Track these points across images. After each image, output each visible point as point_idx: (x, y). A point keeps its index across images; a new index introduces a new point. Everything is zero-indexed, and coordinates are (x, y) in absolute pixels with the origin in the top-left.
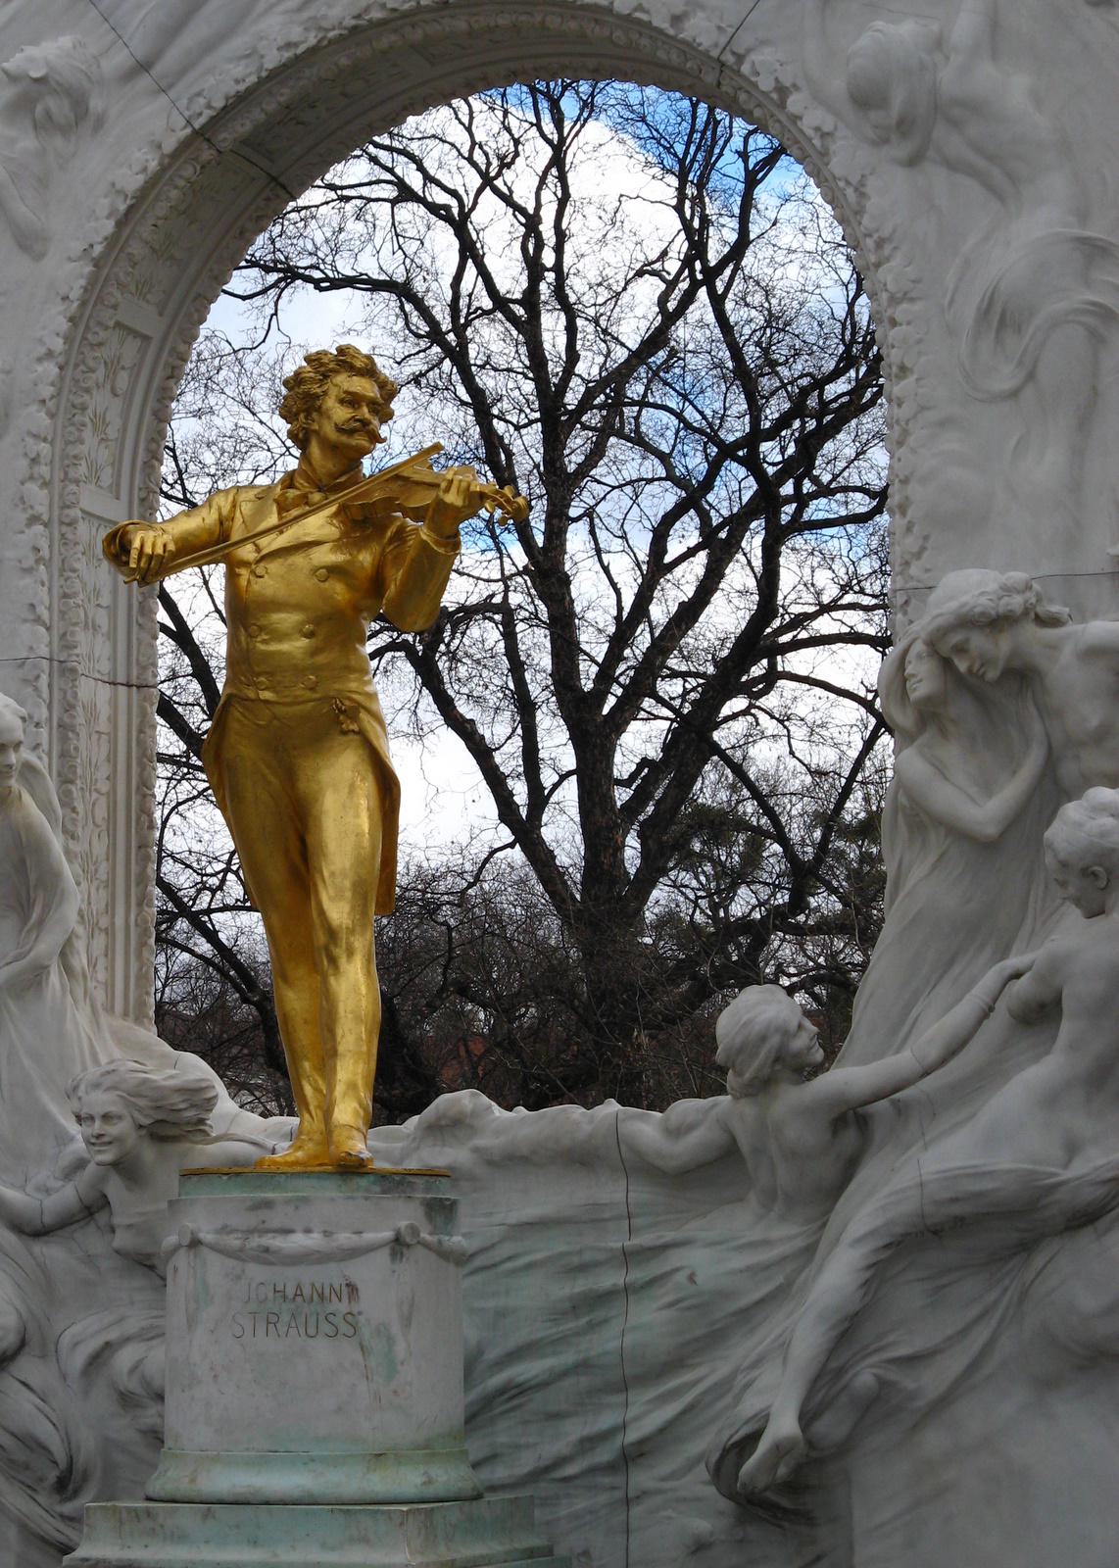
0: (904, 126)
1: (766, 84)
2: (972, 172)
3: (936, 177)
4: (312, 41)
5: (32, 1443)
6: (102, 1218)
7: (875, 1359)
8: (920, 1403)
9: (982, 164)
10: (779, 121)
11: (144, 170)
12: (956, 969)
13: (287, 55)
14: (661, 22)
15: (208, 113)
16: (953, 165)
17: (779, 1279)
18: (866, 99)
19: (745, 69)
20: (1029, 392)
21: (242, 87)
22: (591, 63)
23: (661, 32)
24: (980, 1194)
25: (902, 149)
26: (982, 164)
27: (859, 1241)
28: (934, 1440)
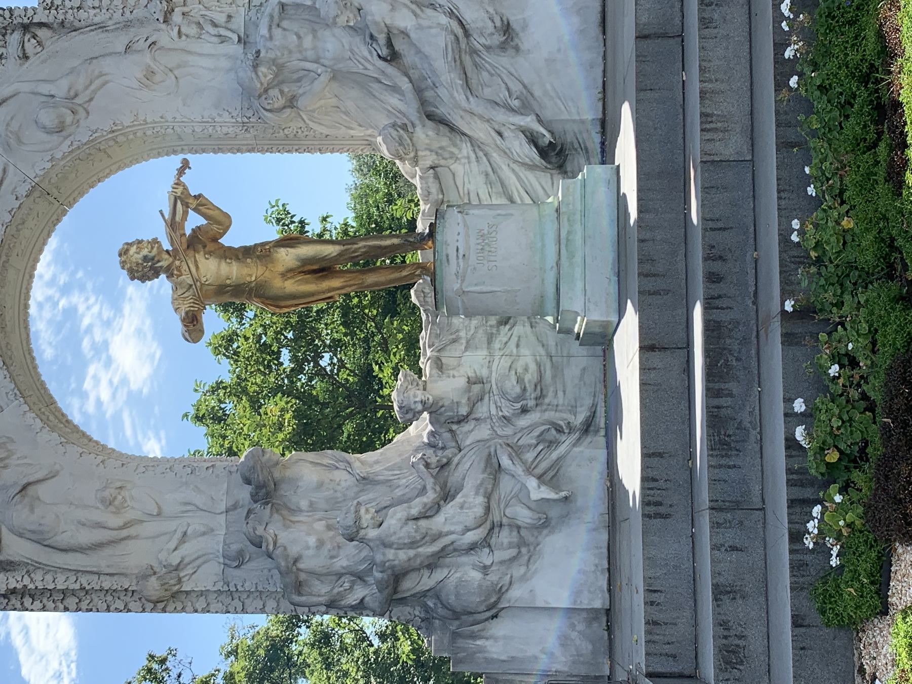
2: (95, 92)
3: (92, 107)
5: (540, 438)
7: (509, 101)
8: (524, 91)
9: (93, 87)
11: (34, 418)
12: (377, 94)
15: (16, 391)
16: (91, 100)
17: (481, 154)
19: (42, 173)
20: (176, 72)
21: (8, 376)
22: (27, 276)
24: (453, 50)
25: (82, 113)
27: (468, 99)
28: (537, 93)
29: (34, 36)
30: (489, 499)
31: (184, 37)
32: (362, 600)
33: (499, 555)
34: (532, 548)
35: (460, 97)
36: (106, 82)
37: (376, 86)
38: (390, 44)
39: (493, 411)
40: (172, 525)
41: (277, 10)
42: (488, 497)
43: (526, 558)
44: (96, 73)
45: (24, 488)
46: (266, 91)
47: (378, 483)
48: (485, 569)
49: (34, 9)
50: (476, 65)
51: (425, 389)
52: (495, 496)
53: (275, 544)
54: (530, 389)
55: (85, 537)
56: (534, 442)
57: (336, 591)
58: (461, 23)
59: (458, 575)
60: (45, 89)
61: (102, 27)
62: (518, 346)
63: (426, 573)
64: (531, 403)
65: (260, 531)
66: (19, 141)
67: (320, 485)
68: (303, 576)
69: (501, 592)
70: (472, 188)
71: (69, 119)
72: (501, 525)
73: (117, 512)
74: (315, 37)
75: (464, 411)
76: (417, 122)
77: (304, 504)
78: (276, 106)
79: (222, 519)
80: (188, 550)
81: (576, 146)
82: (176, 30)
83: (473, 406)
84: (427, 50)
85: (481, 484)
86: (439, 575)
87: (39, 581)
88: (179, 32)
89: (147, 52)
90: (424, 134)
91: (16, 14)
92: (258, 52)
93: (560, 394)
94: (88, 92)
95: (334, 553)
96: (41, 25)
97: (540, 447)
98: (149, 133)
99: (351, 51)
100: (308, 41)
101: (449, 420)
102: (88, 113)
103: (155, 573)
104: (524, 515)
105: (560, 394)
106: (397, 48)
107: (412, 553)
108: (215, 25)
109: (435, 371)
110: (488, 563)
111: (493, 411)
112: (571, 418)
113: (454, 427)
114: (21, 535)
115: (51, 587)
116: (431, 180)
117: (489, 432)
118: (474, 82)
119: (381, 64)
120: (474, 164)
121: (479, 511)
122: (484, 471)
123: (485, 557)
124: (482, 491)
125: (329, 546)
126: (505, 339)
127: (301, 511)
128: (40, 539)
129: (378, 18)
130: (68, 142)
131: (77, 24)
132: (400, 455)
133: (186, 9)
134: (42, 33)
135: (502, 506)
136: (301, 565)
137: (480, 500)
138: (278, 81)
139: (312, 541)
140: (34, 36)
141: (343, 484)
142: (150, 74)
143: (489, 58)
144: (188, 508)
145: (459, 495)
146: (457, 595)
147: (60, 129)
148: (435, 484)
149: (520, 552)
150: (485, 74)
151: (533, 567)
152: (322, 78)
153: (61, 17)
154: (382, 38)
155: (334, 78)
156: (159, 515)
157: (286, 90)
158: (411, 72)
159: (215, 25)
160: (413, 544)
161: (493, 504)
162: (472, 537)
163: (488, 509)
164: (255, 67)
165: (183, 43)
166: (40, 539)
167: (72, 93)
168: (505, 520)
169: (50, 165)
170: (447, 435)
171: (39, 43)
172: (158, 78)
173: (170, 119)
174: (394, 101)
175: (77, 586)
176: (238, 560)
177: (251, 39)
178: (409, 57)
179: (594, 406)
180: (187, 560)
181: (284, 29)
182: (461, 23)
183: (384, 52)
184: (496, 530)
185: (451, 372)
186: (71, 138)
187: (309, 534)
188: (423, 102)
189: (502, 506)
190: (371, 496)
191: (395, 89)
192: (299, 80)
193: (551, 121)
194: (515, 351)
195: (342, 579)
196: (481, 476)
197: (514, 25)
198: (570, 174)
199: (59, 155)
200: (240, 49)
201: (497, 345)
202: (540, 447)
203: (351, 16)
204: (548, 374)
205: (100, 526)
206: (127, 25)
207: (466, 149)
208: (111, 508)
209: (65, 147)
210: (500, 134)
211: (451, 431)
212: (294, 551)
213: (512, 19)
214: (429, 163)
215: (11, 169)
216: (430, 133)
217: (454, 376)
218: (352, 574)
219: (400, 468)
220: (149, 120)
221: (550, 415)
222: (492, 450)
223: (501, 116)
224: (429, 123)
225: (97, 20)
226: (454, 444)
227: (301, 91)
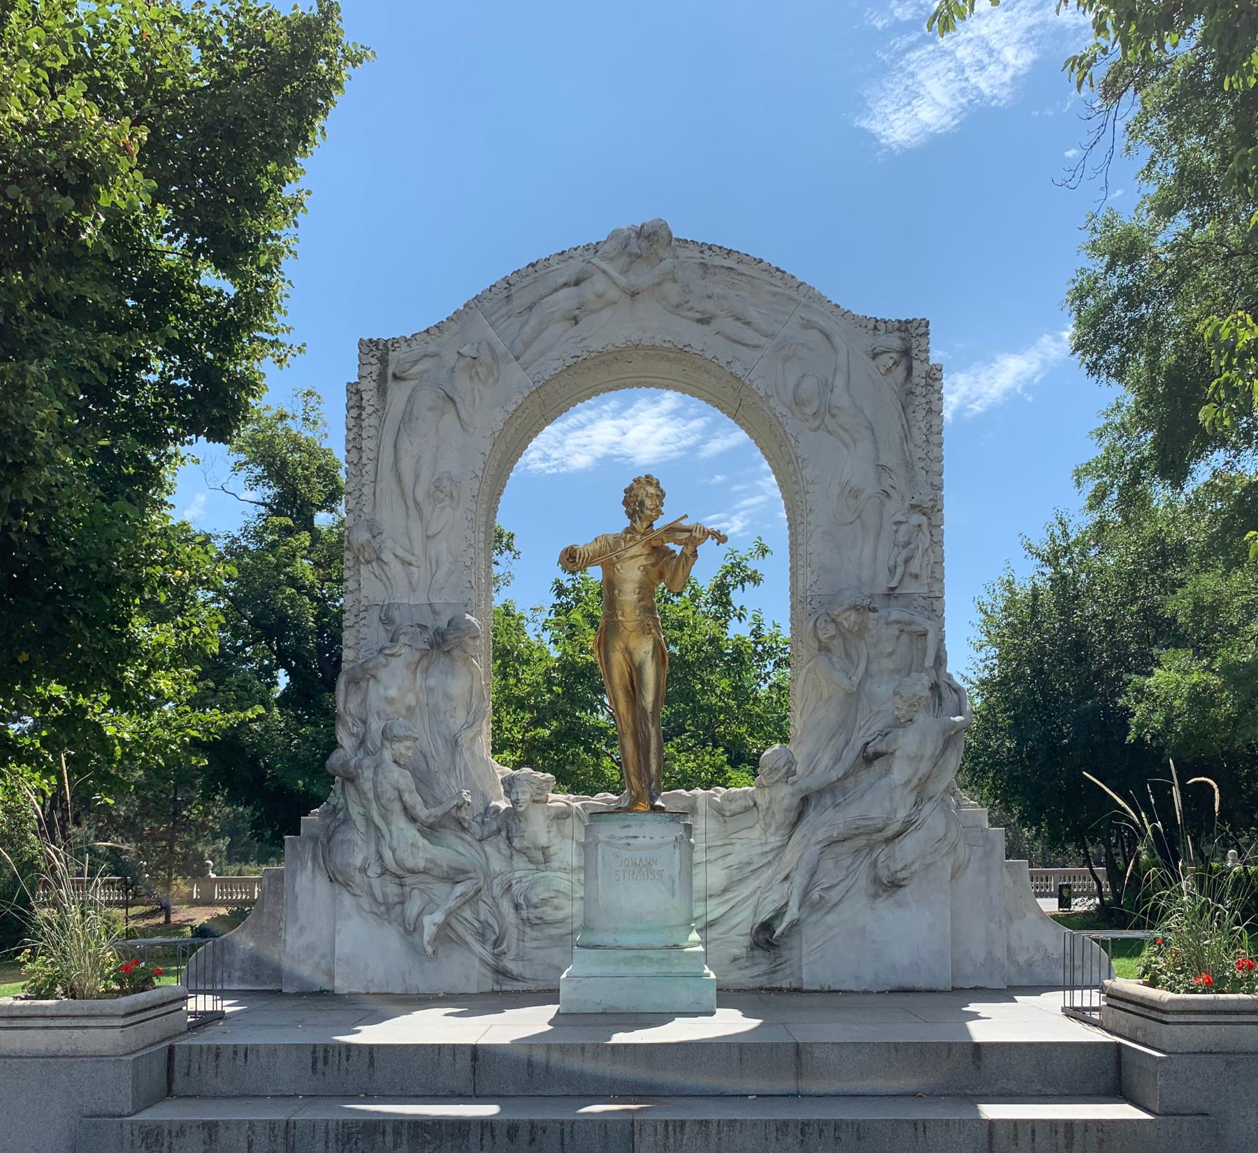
6: (504, 833)
30: (424, 872)
33: (376, 883)
35: (821, 835)
37: (842, 740)
38: (878, 755)
40: (418, 551)
41: (919, 628)
42: (425, 872)
46: (834, 621)
47: (453, 755)
50: (858, 851)
51: (535, 801)
52: (429, 879)
53: (392, 655)
54: (538, 912)
55: (407, 465)
57: (349, 719)
58: (898, 835)
59: (360, 842)
64: (524, 913)
65: (403, 639)
67: (448, 697)
68: (363, 684)
70: (737, 847)
71: (809, 410)
73: (430, 495)
74: (892, 671)
76: (796, 787)
77: (432, 682)
78: (820, 632)
79: (424, 601)
80: (395, 568)
82: (902, 519)
83: (523, 852)
84: (868, 797)
85: (436, 865)
87: (370, 421)
90: (785, 795)
92: (875, 610)
95: (383, 716)
98: (797, 497)
99: (878, 712)
100: (888, 664)
101: (507, 826)
103: (374, 537)
104: (413, 908)
106: (876, 763)
107: (371, 795)
109: (553, 811)
111: (517, 874)
113: (504, 833)
116: (743, 803)
117: (497, 869)
118: (838, 849)
119: (859, 745)
120: (759, 850)
121: (410, 863)
122: (450, 867)
123: (374, 870)
124: (430, 865)
125: (389, 709)
127: (426, 679)
128: (407, 419)
129: (901, 741)
131: (911, 408)
132: (479, 777)
135: (421, 886)
137: (421, 864)
138: (842, 633)
139: (393, 693)
141: (452, 720)
142: (855, 494)
143: (864, 867)
145: (426, 842)
146: (343, 841)
147: (799, 402)
148: (436, 817)
150: (848, 861)
152: (846, 681)
153: (918, 390)
154: (882, 747)
155: (848, 695)
156: (428, 537)
157: (835, 642)
158: (852, 779)
160: (378, 797)
161: (421, 877)
163: (413, 872)
164: (856, 608)
166: (407, 419)
168: (407, 889)
169: (762, 394)
170: (494, 827)
174: (826, 760)
176: (387, 621)
177: (893, 602)
178: (867, 776)
181: (898, 638)
182: (898, 835)
183: (870, 750)
185: (554, 829)
187: (399, 689)
188: (820, 792)
190: (441, 749)
191: (838, 759)
192: (848, 655)
195: (361, 724)
196: (444, 864)
197: (901, 892)
200: (882, 588)
203: (903, 712)
206: (908, 465)
207: (775, 841)
208: (433, 489)
210: (786, 878)
211: (499, 831)
212: (383, 674)
213: (907, 890)
214: (759, 801)
215: (758, 354)
216: (786, 802)
217: (549, 832)
218: (364, 735)
219: (467, 779)
221: (513, 933)
223: (799, 879)
224: (796, 800)
226: (486, 833)
227: (835, 659)
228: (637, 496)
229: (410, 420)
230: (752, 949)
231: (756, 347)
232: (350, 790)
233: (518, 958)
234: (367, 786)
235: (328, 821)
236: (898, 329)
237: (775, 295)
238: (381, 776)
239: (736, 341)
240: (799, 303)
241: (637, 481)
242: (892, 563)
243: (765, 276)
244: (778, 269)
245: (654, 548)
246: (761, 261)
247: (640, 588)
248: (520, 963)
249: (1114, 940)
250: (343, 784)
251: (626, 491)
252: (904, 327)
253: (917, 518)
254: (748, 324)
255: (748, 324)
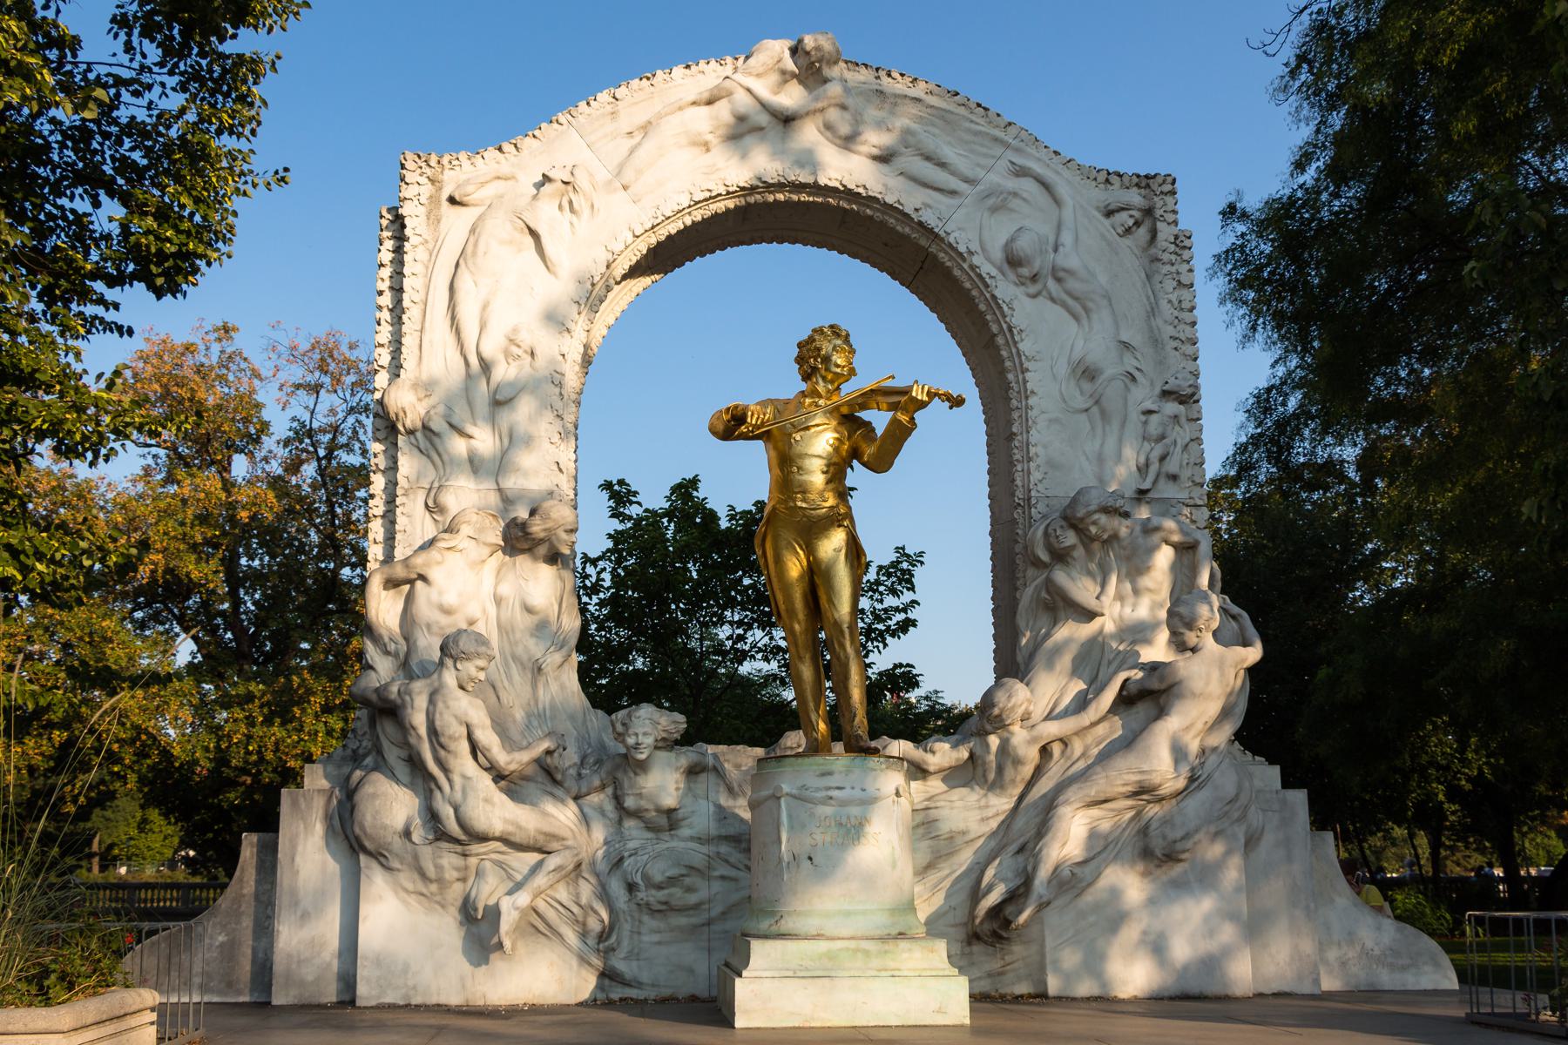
0: (1034, 278)
1: (962, 249)
2: (1064, 305)
4: (723, 190)
9: (1070, 302)
10: (962, 269)
13: (707, 195)
14: (909, 210)
16: (1053, 300)
18: (1013, 261)
19: (952, 240)
23: (906, 215)
25: (1033, 289)
26: (1070, 302)
29: (1137, 224)
31: (1143, 418)
32: (371, 668)
34: (438, 898)
36: (1076, 317)
39: (631, 845)
43: (424, 891)
44: (1090, 305)
45: (534, 234)
48: (407, 833)
49: (1175, 223)
56: (584, 901)
60: (1067, 238)
61: (1153, 311)
62: (723, 878)
63: (404, 754)
64: (641, 895)
66: (994, 210)
69: (378, 856)
72: (465, 855)
75: (630, 802)
81: (1008, 958)
83: (636, 814)
86: (402, 770)
88: (1150, 412)
89: (1120, 370)
91: (1169, 199)
93: (656, 938)
94: (1065, 297)
96: (1154, 233)
97: (575, 909)
102: (1034, 296)
105: (656, 938)
108: (1163, 458)
110: (415, 837)
112: (622, 953)
114: (473, 231)
115: (406, 271)
126: (732, 860)
130: (994, 272)
133: (1183, 420)
134: (1142, 233)
135: (494, 856)
136: (419, 584)
140: (1137, 224)
144: (506, 441)
149: (431, 881)
151: (412, 900)
159: (1163, 458)
162: (447, 812)
165: (1135, 417)
167: (1061, 274)
171: (1128, 231)
172: (1087, 386)
173: (1030, 402)
175: (406, 303)
179: (637, 984)
180: (436, 440)
184: (459, 848)
186: (1000, 277)
189: (494, 856)
193: (1042, 923)
194: (716, 873)
198: (967, 950)
199: (976, 260)
201: (724, 849)
202: (575, 909)
204: (682, 921)
205: (483, 327)
206: (1156, 341)
209: (986, 269)
215: (954, 201)
220: (1028, 375)
222: (569, 843)
225: (1163, 304)
228: (819, 349)
229: (474, 253)
230: (969, 944)
231: (953, 193)
232: (387, 728)
233: (633, 955)
234: (419, 720)
235: (346, 770)
236: (1137, 185)
237: (977, 133)
238: (440, 705)
239: (926, 185)
240: (1007, 146)
241: (819, 331)
242: (1142, 460)
243: (962, 110)
244: (979, 105)
245: (844, 416)
246: (957, 94)
247: (828, 465)
248: (634, 964)
249: (1491, 918)
250: (372, 723)
251: (800, 345)
252: (1145, 182)
253: (1172, 407)
254: (942, 165)
255: (942, 165)
